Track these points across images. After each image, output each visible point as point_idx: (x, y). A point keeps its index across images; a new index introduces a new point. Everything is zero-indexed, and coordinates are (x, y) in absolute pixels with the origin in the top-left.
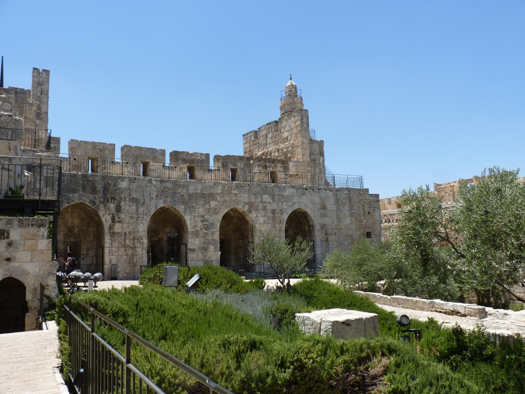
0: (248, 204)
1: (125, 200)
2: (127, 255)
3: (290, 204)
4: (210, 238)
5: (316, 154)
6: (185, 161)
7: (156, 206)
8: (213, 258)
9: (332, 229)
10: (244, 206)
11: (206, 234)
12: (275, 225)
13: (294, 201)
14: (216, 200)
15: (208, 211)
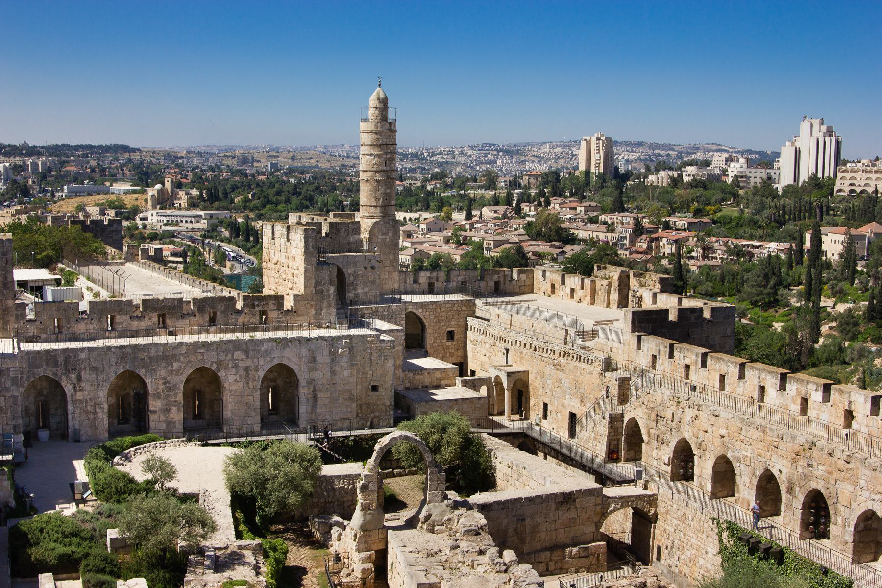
0: (216, 362)
1: (85, 370)
2: (88, 420)
3: (268, 359)
4: (173, 399)
5: (325, 284)
6: (154, 309)
7: (116, 373)
8: (176, 419)
9: (323, 384)
10: (212, 364)
11: (169, 396)
12: (248, 383)
13: (273, 356)
14: (179, 361)
15: (171, 372)
